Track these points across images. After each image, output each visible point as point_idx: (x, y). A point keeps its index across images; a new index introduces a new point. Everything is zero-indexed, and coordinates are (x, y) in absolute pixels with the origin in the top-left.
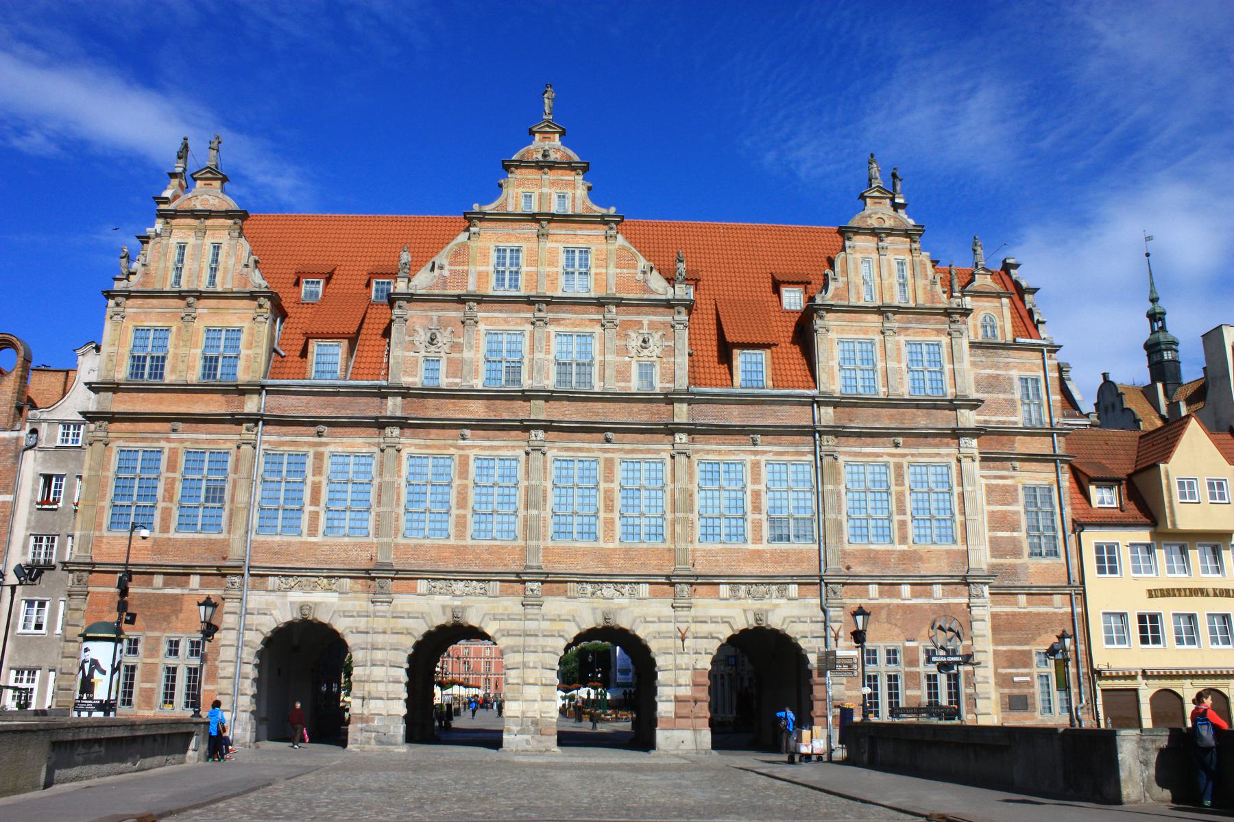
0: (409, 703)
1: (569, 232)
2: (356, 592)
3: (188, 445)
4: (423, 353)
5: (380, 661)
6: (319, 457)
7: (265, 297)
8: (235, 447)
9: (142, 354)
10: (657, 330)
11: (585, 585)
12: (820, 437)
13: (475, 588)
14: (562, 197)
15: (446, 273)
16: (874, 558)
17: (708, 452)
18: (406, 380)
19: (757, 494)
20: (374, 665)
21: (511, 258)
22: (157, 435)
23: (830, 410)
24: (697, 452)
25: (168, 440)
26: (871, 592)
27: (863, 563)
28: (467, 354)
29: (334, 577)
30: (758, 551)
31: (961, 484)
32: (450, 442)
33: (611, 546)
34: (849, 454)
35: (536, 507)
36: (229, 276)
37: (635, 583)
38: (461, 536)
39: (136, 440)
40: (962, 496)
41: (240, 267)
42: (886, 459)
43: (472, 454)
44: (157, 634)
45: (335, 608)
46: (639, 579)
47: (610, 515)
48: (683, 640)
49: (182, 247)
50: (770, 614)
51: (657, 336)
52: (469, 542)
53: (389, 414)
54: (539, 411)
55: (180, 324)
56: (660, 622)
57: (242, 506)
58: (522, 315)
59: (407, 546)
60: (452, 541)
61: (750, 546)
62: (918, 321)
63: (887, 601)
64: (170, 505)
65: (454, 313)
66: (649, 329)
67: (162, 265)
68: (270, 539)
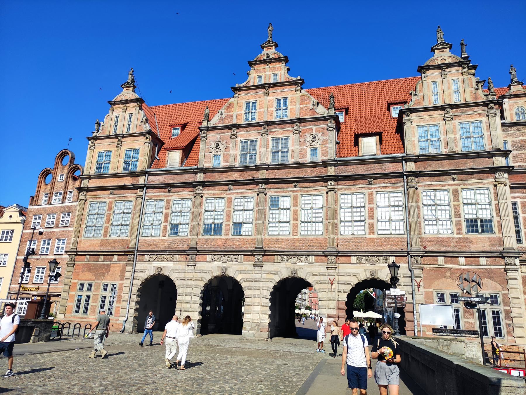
2: (180, 261)
3: (117, 199)
4: (213, 153)
5: (189, 293)
6: (168, 201)
7: (148, 134)
8: (135, 199)
9: (101, 162)
10: (320, 132)
11: (283, 257)
12: (407, 178)
13: (233, 258)
14: (275, 75)
15: (223, 116)
16: (441, 241)
17: (345, 189)
18: (206, 165)
20: (186, 295)
21: (252, 106)
23: (413, 163)
24: (340, 189)
26: (439, 261)
27: (434, 245)
29: (171, 254)
30: (372, 238)
31: (497, 199)
32: (224, 192)
33: (296, 237)
34: (425, 186)
35: (261, 220)
36: (135, 126)
37: (307, 255)
38: (227, 234)
39: (96, 198)
41: (139, 122)
42: (447, 187)
43: (233, 196)
44: (99, 282)
45: (171, 269)
46: (309, 253)
47: (295, 222)
48: (332, 285)
49: (117, 117)
50: (379, 272)
51: (319, 135)
52: (230, 237)
53: (198, 181)
54: (263, 175)
55: (116, 149)
56: (320, 275)
58: (257, 131)
60: (223, 237)
61: (368, 236)
62: (466, 111)
63: (451, 266)
64: (108, 225)
65: (227, 134)
66: (316, 132)
67: (109, 125)
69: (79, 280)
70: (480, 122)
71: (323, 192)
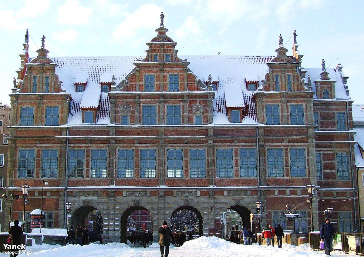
0: (121, 232)
1: (171, 69)
6: (88, 151)
12: (259, 140)
13: (142, 194)
17: (220, 146)
19: (236, 160)
22: (32, 145)
24: (216, 146)
25: (36, 147)
28: (137, 114)
31: (308, 156)
32: (132, 145)
33: (187, 179)
34: (269, 146)
40: (308, 160)
42: (282, 147)
43: (140, 149)
48: (212, 210)
50: (241, 201)
51: (202, 106)
52: (140, 179)
57: (63, 168)
59: (119, 180)
61: (234, 178)
63: (282, 196)
66: (199, 103)
67: (29, 85)
68: (73, 179)
69: (19, 210)
70: (302, 106)
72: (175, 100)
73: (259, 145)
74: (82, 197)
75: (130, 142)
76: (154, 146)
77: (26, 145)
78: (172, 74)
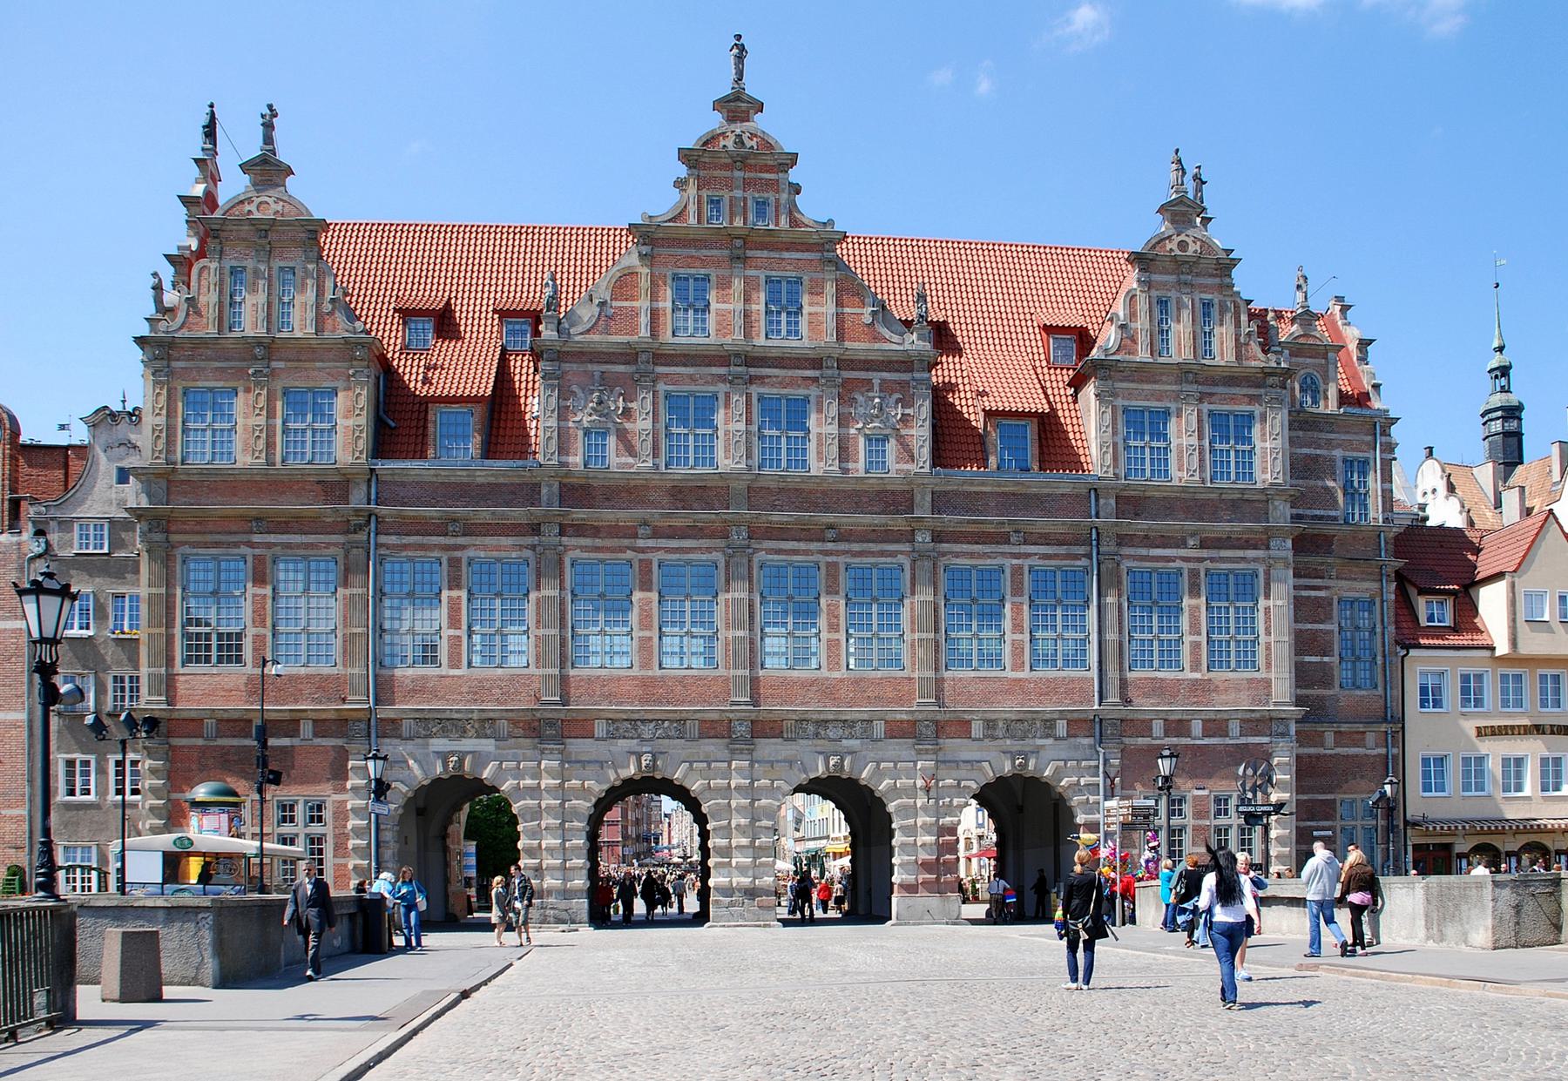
1: (773, 254)
6: (454, 564)
12: (1098, 534)
17: (957, 555)
24: (944, 554)
25: (251, 545)
27: (1147, 695)
30: (1020, 680)
32: (626, 542)
33: (836, 675)
35: (740, 627)
38: (645, 665)
39: (206, 545)
42: (1178, 564)
43: (655, 557)
47: (836, 636)
52: (659, 673)
57: (359, 630)
60: (635, 672)
61: (1009, 674)
64: (261, 631)
66: (881, 391)
71: (901, 558)
72: (790, 373)
73: (1098, 553)
74: (432, 741)
75: (615, 531)
76: (709, 550)
77: (209, 538)
78: (780, 274)
